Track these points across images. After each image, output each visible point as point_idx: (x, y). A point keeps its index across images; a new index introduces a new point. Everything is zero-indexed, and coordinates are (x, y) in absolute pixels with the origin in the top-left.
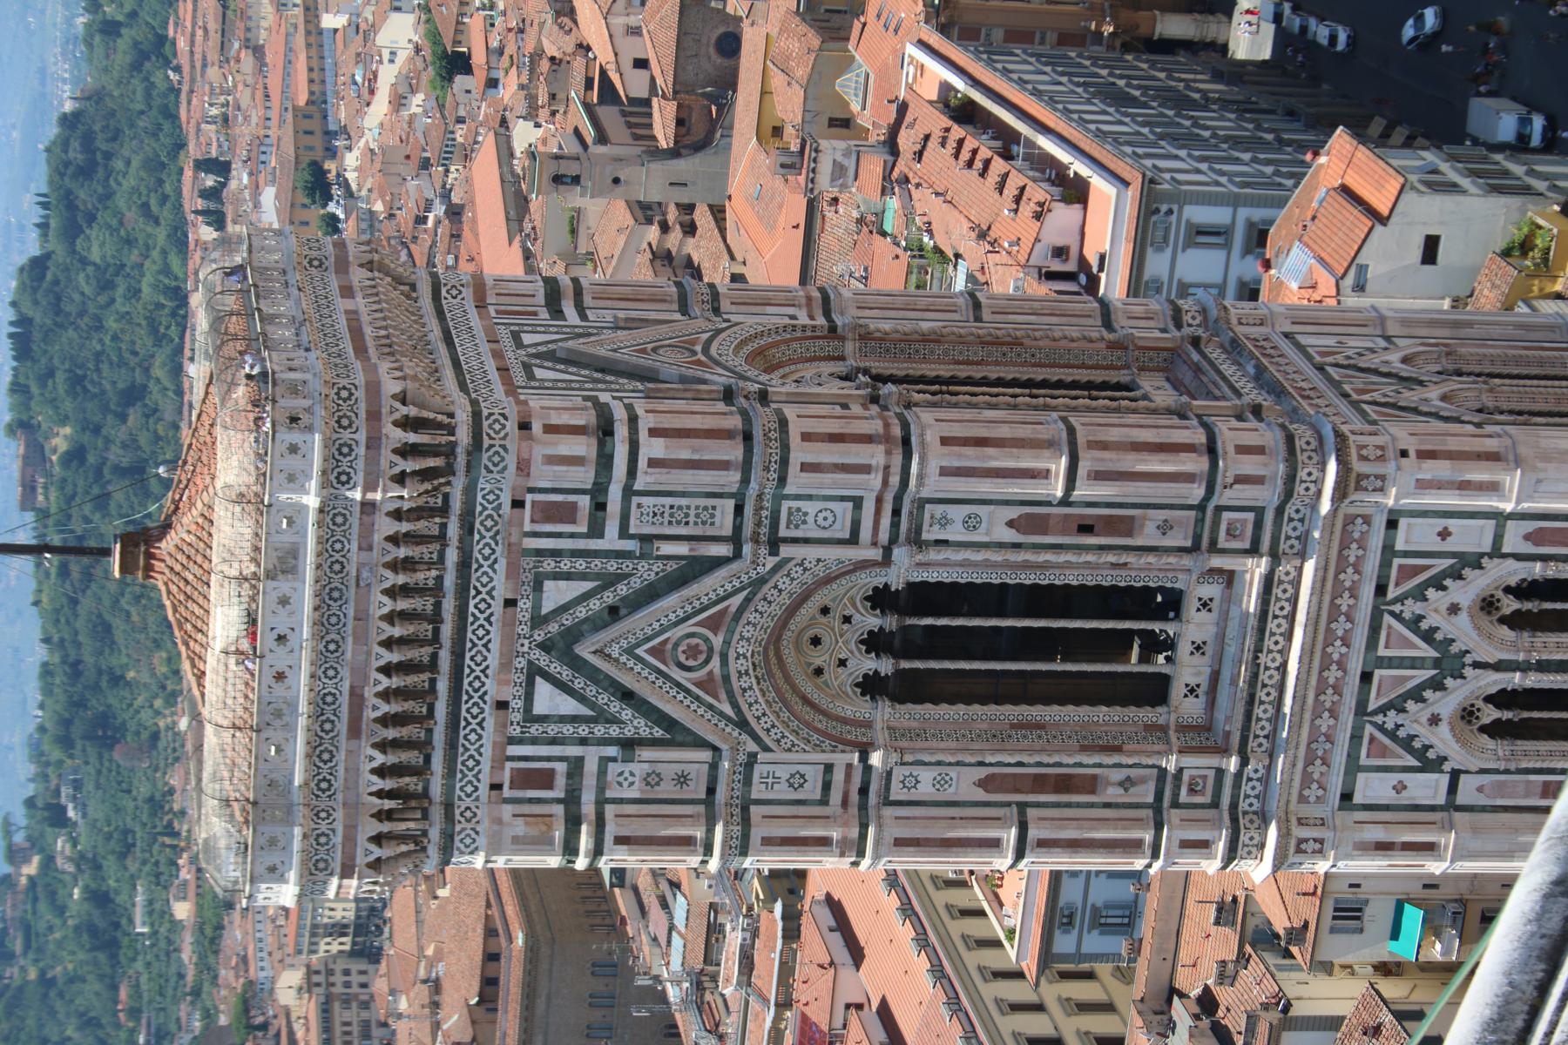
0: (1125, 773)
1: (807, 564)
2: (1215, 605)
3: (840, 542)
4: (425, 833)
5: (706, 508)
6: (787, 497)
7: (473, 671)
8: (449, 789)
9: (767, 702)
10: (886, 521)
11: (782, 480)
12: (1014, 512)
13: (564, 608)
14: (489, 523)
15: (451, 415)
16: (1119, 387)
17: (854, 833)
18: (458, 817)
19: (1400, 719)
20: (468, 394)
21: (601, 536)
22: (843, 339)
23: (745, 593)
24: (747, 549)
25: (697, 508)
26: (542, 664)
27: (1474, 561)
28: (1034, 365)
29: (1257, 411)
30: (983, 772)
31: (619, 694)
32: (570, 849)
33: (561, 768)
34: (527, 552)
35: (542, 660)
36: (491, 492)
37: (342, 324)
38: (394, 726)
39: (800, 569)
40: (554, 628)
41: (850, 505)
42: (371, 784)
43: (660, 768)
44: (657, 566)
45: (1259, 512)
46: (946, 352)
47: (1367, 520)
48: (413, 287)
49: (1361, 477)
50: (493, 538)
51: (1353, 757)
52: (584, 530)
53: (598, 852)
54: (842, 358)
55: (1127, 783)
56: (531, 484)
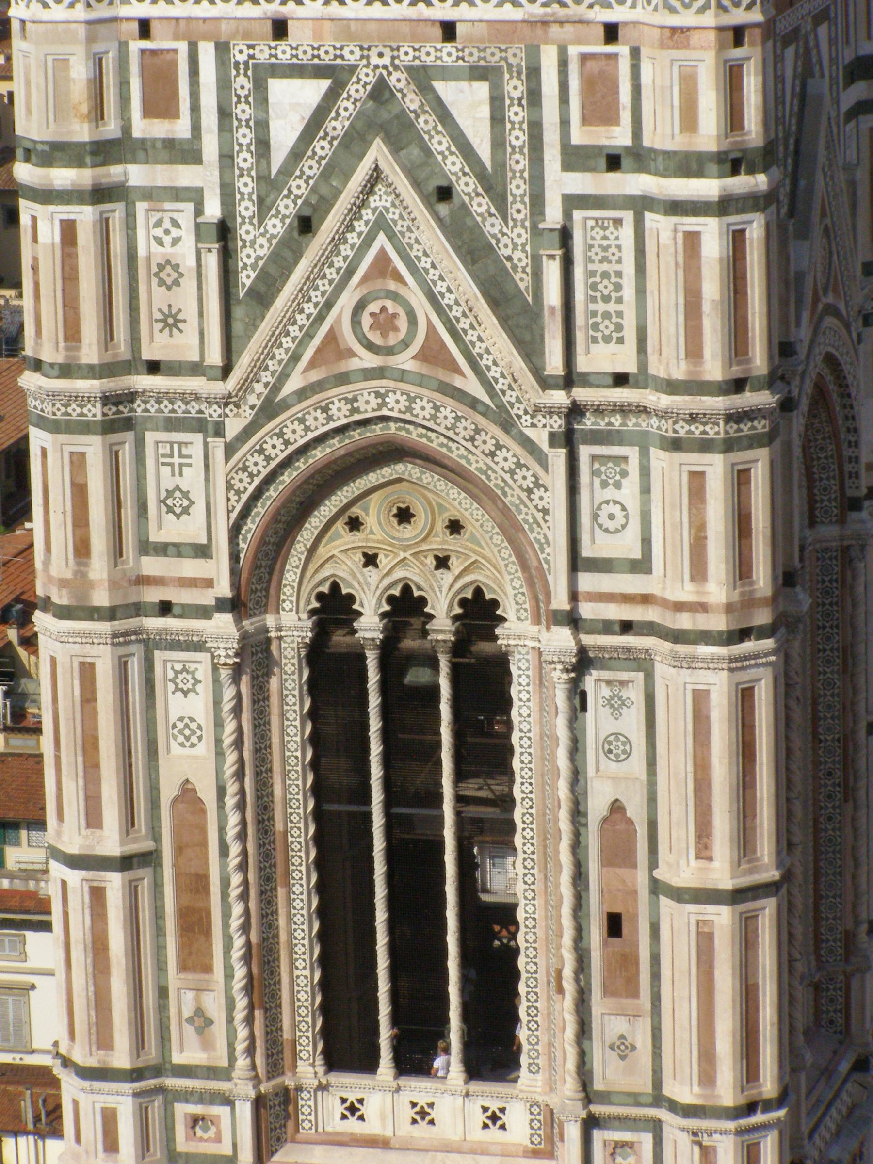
1: (538, 493)
2: (494, 1133)
5: (619, 328)
6: (645, 454)
11: (676, 445)
12: (636, 811)
13: (444, 116)
17: (101, 598)
21: (567, 166)
22: (842, 521)
23: (486, 399)
24: (559, 398)
25: (620, 314)
26: (352, 88)
30: (208, 794)
31: (307, 212)
33: (181, 128)
34: (533, 53)
39: (529, 482)
40: (412, 102)
41: (637, 555)
54: (812, 522)
56: (644, 52)
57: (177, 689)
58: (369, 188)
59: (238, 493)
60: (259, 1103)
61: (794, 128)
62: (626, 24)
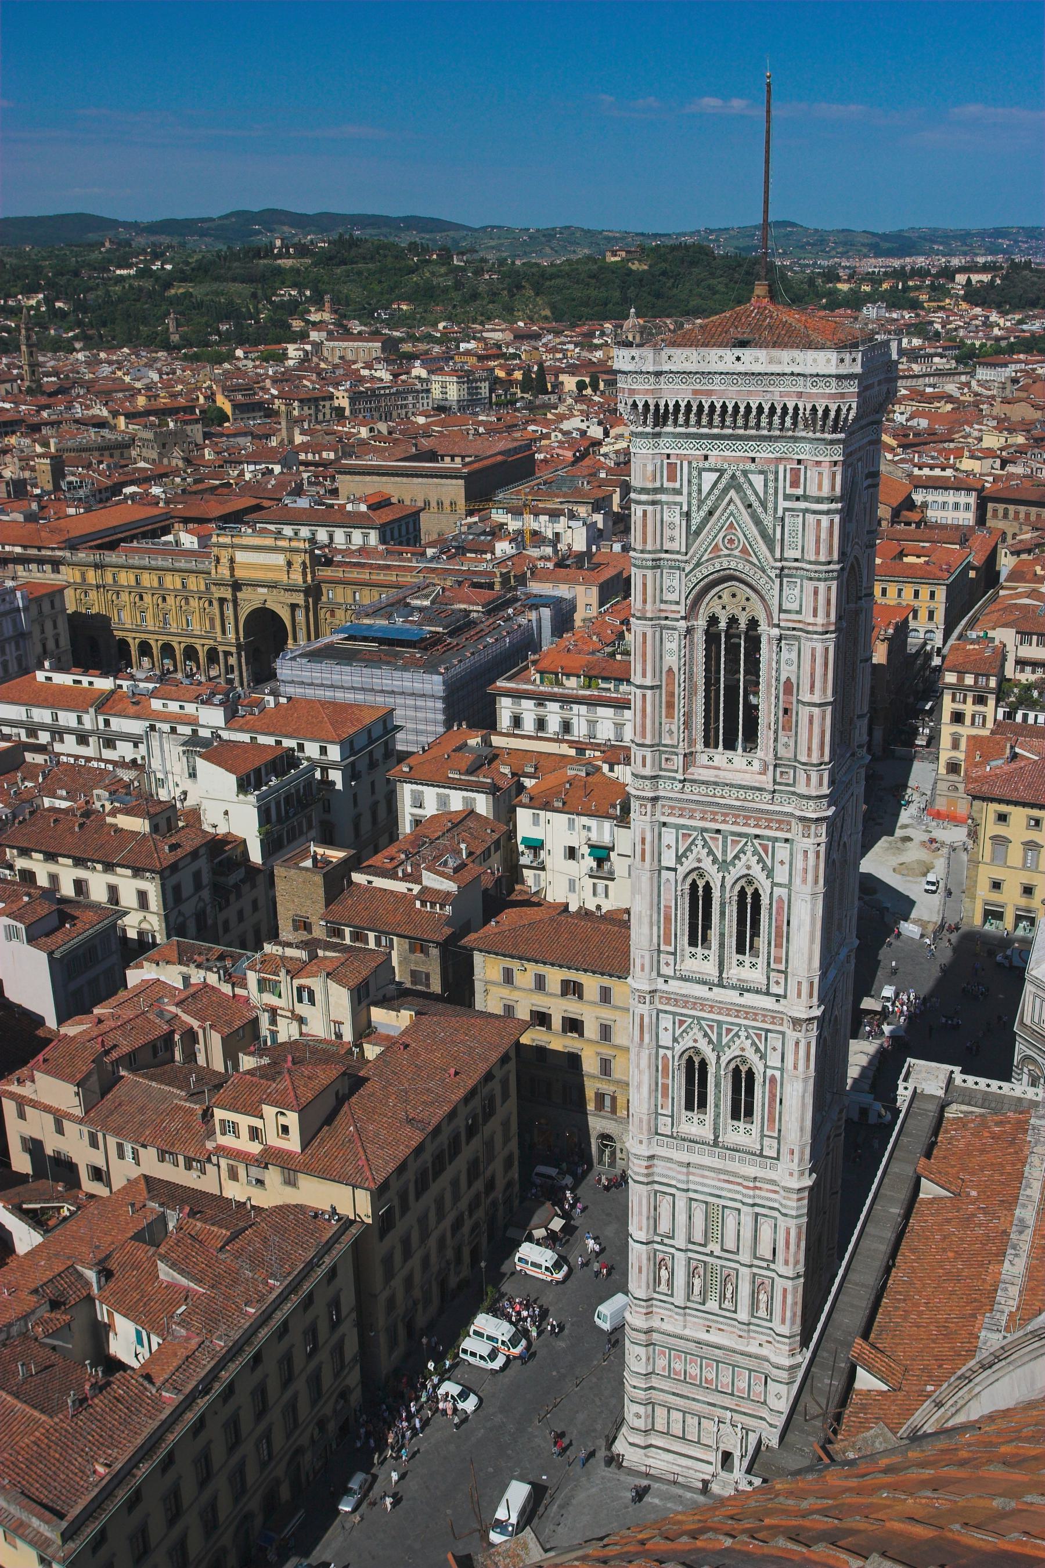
3: (780, 605)
10: (791, 625)
11: (811, 579)
12: (794, 680)
13: (751, 484)
17: (649, 615)
19: (700, 847)
24: (779, 564)
27: (770, 875)
30: (676, 670)
32: (643, 491)
33: (677, 485)
34: (777, 467)
35: (727, 476)
40: (742, 480)
44: (770, 525)
45: (793, 785)
47: (789, 831)
49: (809, 827)
51: (683, 827)
53: (639, 503)
55: (670, 732)
58: (729, 504)
60: (685, 755)
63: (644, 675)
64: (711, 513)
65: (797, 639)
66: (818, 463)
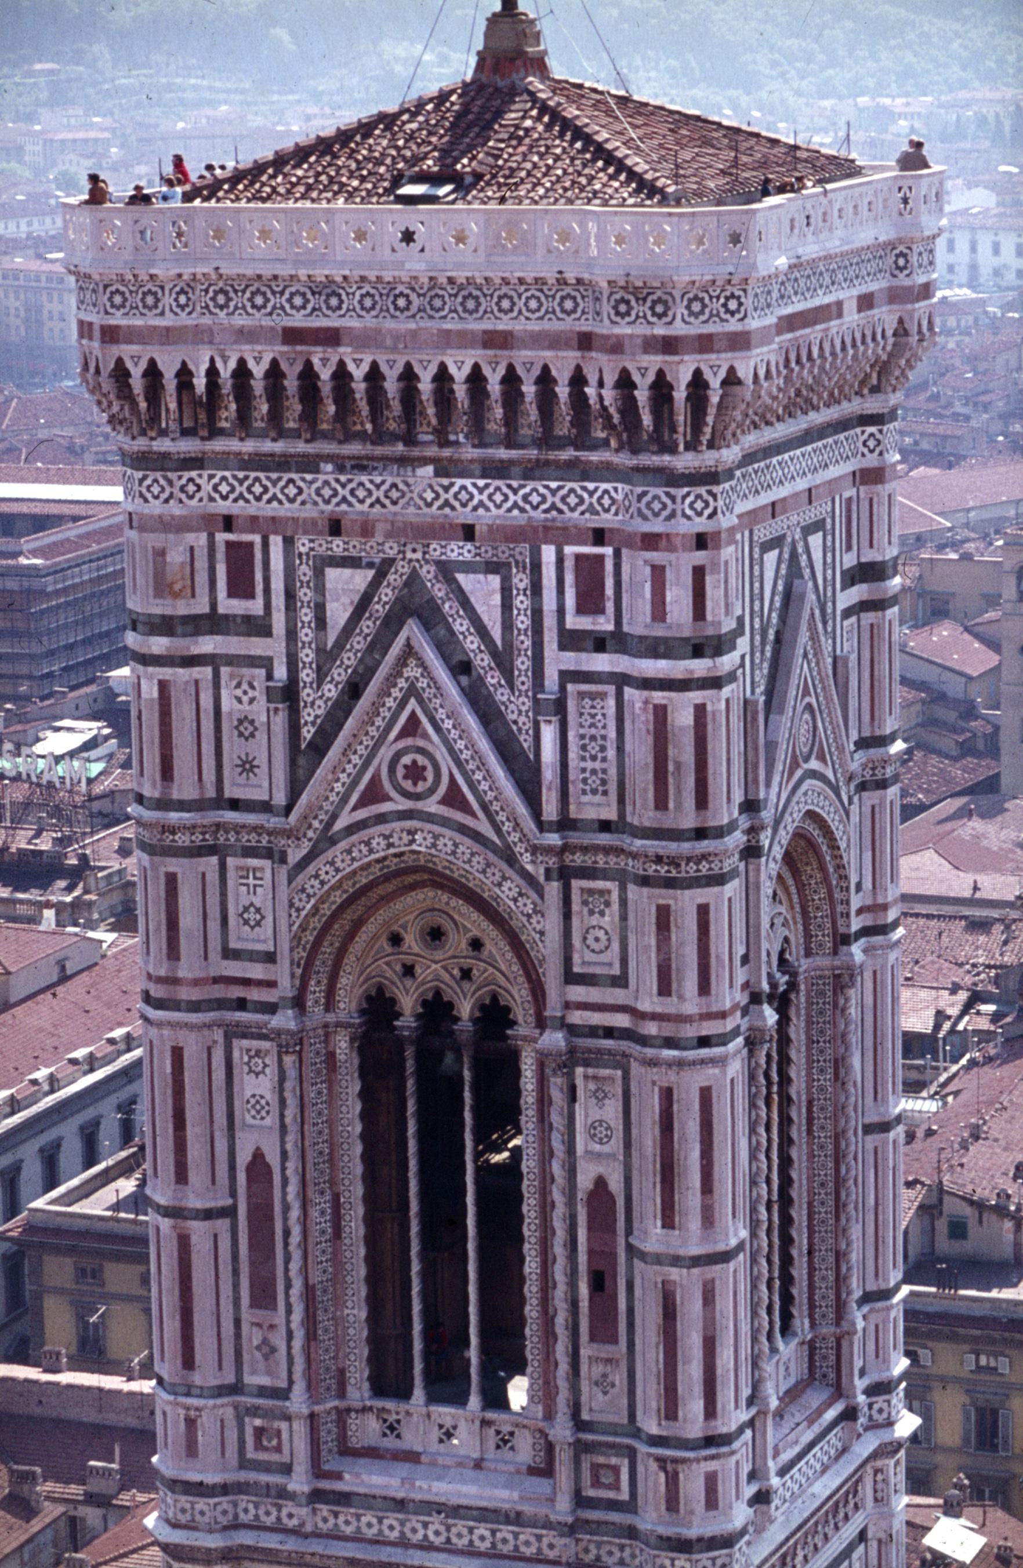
0: (281, 1344)
3: (568, 961)
4: (163, 433)
5: (604, 782)
6: (623, 889)
7: (378, 487)
8: (223, 461)
9: (354, 873)
10: (596, 1019)
11: (645, 881)
12: (616, 1184)
13: (465, 602)
14: (572, 500)
15: (711, 445)
16: (787, 1318)
18: (187, 475)
20: (740, 466)
21: (562, 647)
22: (835, 952)
23: (496, 839)
24: (554, 839)
25: (604, 771)
26: (391, 577)
28: (810, 1204)
29: (762, 1498)
30: (273, 1159)
31: (357, 679)
33: (255, 607)
36: (613, 501)
37: (822, 299)
38: (301, 388)
39: (529, 909)
41: (616, 971)
42: (225, 360)
43: (261, 736)
44: (525, 722)
45: (630, 1506)
46: (822, 1089)
48: (876, 390)
50: (553, 507)
52: (569, 625)
54: (808, 953)
57: (251, 1071)
58: (402, 662)
59: (298, 910)
61: (775, 620)
62: (611, 530)
63: (181, 1176)
64: (354, 690)
65: (622, 1062)
66: (651, 541)
